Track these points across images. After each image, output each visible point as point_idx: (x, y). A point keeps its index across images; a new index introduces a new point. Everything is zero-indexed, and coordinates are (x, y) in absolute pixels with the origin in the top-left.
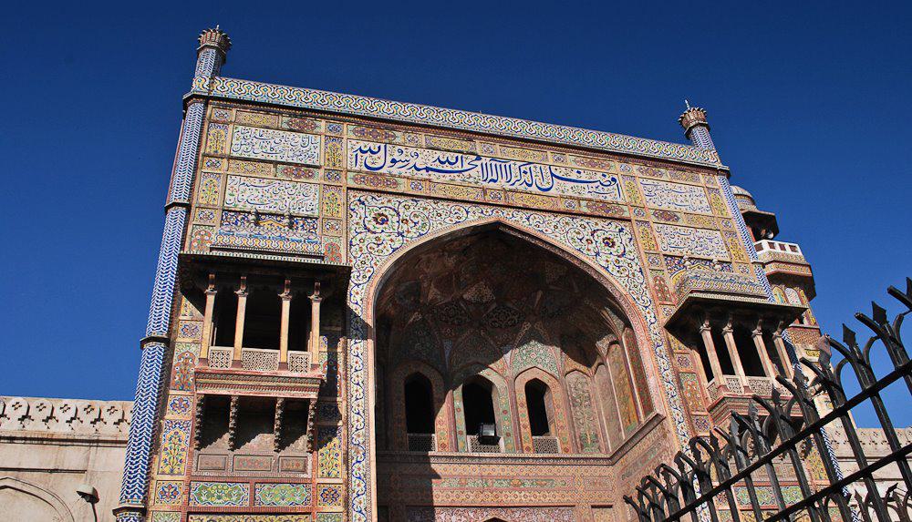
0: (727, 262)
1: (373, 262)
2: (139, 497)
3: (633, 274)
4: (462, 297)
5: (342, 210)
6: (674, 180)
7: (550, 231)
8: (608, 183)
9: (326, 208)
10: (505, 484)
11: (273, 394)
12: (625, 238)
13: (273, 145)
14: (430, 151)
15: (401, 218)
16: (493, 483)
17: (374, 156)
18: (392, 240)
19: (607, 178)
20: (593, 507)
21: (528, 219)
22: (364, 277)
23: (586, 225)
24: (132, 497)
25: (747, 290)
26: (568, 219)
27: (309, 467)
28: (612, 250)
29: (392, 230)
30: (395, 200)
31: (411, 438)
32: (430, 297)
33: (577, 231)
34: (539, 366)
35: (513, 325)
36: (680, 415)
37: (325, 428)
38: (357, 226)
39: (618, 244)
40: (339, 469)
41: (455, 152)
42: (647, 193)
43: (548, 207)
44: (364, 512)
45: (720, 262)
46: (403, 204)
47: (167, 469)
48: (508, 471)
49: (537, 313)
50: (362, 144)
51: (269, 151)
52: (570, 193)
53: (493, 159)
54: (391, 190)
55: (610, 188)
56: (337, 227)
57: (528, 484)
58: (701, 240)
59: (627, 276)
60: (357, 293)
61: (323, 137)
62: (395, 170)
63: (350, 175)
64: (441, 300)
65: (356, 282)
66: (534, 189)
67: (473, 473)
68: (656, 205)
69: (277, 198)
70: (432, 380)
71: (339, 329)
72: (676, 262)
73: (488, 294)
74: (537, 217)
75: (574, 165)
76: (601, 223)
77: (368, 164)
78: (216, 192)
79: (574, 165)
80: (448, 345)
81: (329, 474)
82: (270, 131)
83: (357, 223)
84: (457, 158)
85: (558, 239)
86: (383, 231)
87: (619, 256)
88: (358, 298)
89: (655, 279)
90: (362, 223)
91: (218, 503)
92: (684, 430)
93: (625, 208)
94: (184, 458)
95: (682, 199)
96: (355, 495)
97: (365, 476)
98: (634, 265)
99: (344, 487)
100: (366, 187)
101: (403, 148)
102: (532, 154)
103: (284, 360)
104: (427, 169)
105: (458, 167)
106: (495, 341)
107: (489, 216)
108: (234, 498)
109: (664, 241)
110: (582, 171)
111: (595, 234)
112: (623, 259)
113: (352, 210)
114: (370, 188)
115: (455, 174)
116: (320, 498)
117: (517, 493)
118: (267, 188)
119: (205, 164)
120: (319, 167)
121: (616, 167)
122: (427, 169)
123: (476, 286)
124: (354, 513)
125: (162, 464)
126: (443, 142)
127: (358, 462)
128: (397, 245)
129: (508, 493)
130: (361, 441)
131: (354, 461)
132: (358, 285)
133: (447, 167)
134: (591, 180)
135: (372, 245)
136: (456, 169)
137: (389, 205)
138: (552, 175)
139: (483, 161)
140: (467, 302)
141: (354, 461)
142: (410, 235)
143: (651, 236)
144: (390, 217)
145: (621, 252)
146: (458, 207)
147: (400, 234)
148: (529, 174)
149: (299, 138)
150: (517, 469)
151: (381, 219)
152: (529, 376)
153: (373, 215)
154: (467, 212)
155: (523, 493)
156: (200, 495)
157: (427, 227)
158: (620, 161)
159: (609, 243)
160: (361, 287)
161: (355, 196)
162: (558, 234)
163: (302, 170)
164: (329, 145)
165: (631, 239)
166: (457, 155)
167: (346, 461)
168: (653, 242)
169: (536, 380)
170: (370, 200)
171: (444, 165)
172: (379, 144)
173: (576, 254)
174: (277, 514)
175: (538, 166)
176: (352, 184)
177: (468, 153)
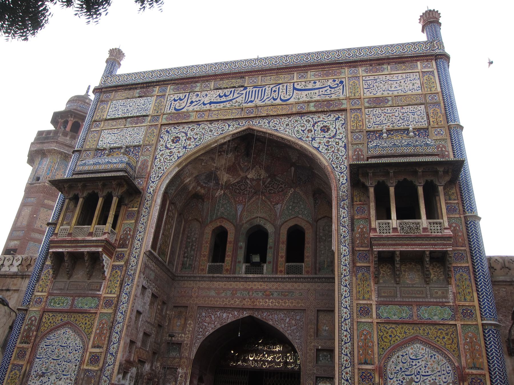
0: (423, 129)
1: (165, 167)
2: (26, 303)
3: (338, 150)
4: (246, 177)
5: (155, 139)
7: (282, 128)
8: (336, 85)
9: (147, 139)
10: (260, 294)
11: (82, 250)
12: (338, 124)
13: (129, 107)
14: (215, 91)
15: (188, 137)
16: (253, 293)
17: (181, 102)
18: (179, 152)
19: (336, 82)
20: (318, 311)
21: (269, 123)
23: (310, 119)
24: (24, 303)
25: (420, 150)
26: (298, 118)
27: (102, 288)
28: (326, 135)
29: (180, 146)
30: (187, 126)
31: (210, 266)
32: (225, 179)
33: (302, 125)
34: (300, 216)
35: (282, 191)
36: (347, 251)
37: (115, 266)
38: (161, 147)
40: (117, 289)
41: (230, 88)
42: (365, 87)
43: (284, 112)
44: (124, 313)
45: (418, 130)
46: (191, 128)
47: (40, 290)
48: (264, 286)
49: (294, 181)
50: (176, 96)
51: (126, 112)
52: (305, 99)
53: (255, 87)
54: (187, 121)
55: (338, 88)
56: (150, 149)
57: (275, 294)
58: (405, 114)
59: (333, 152)
60: (152, 187)
61: (155, 97)
62: (191, 108)
63: (165, 116)
64: (233, 180)
65: (153, 180)
66: (278, 101)
67: (242, 287)
68: (372, 94)
69: (124, 138)
70: (228, 230)
71: (136, 209)
72: (377, 136)
73: (263, 174)
74: (276, 120)
75: (313, 78)
76: (322, 116)
78: (95, 141)
79: (313, 78)
80: (240, 208)
81: (111, 291)
82: (129, 100)
83: (162, 145)
84: (231, 92)
85: (287, 133)
86: (175, 147)
87: (330, 138)
88: (152, 189)
89: (355, 150)
90: (165, 145)
91: (58, 307)
92: (347, 262)
93: (344, 102)
94: (48, 284)
95: (397, 85)
96: (122, 303)
97: (129, 293)
98: (340, 142)
99: (116, 299)
100: (171, 122)
101: (199, 93)
102: (283, 78)
103: (91, 231)
104: (210, 103)
106: (271, 202)
107: (243, 126)
108: (65, 305)
109: (372, 121)
110: (317, 81)
111: (316, 125)
112: (332, 140)
114: (173, 122)
115: (227, 103)
116: (104, 305)
117: (267, 300)
118: (119, 134)
119: (93, 127)
120: (147, 116)
121: (346, 72)
122: (210, 103)
123: (254, 169)
124: (119, 313)
125: (39, 287)
126: (225, 83)
127: (128, 285)
128: (181, 154)
129: (261, 300)
130: (132, 273)
131: (126, 285)
132: (153, 182)
133: (224, 99)
134: (324, 86)
135: (167, 156)
136: (228, 99)
137: (183, 130)
138: (294, 89)
139: (248, 90)
140: (252, 180)
141: (126, 285)
142: (190, 147)
143: (360, 119)
144: (181, 138)
145: (332, 135)
146: (224, 124)
147: (185, 147)
148: (277, 92)
149: (142, 100)
150: (270, 285)
151: (176, 140)
152: (291, 224)
153: (172, 138)
154: (229, 126)
155: (271, 300)
156: (50, 303)
157: (202, 140)
158: (350, 67)
159: (325, 129)
160: (154, 183)
161: (164, 129)
162: (288, 130)
163: (139, 118)
164: (158, 101)
166: (231, 89)
167: (121, 285)
168: (361, 124)
169: (296, 226)
170: (172, 129)
171: (222, 98)
172: (185, 94)
173: (297, 141)
174: (82, 313)
175: (285, 85)
176: (164, 122)
177: (239, 87)
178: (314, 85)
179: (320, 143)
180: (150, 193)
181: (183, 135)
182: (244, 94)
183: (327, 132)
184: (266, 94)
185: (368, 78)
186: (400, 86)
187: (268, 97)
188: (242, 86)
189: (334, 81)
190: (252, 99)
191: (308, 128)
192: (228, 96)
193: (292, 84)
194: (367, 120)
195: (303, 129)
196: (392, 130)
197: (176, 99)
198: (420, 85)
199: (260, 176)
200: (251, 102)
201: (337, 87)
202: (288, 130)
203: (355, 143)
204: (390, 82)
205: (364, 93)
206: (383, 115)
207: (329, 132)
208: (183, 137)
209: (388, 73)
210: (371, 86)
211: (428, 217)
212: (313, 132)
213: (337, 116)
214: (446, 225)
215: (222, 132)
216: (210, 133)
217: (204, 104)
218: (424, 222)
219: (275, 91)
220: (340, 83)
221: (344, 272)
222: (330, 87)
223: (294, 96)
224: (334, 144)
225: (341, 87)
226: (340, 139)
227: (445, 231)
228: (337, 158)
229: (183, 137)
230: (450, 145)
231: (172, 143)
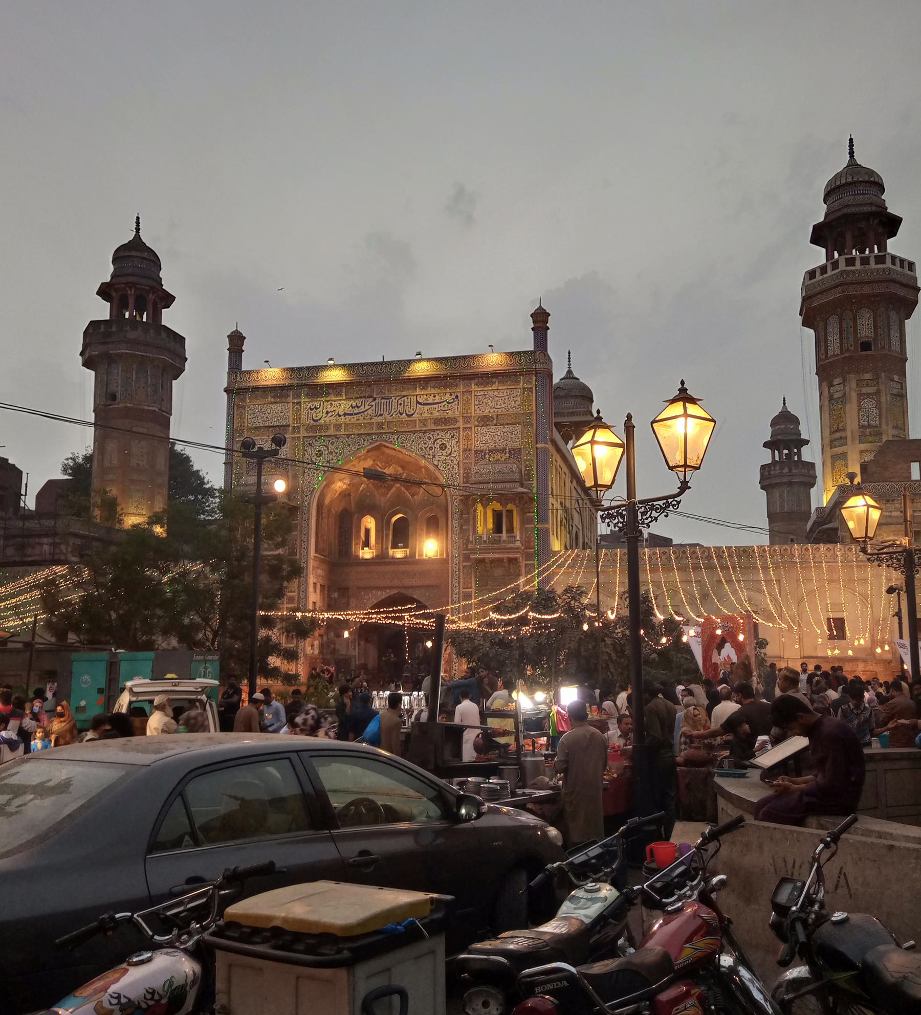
0: (517, 449)
3: (453, 468)
6: (500, 388)
7: (409, 445)
21: (397, 439)
22: (310, 491)
23: (431, 437)
39: (449, 447)
42: (476, 403)
52: (426, 415)
53: (383, 398)
58: (505, 434)
62: (327, 419)
68: (481, 412)
75: (433, 391)
76: (441, 433)
77: (314, 418)
85: (413, 450)
87: (447, 456)
88: (306, 503)
89: (465, 469)
95: (501, 402)
98: (455, 460)
104: (345, 414)
105: (362, 409)
109: (479, 439)
113: (306, 450)
115: (360, 415)
122: (345, 414)
136: (361, 411)
137: (324, 444)
138: (418, 402)
139: (377, 401)
145: (449, 452)
149: (278, 407)
154: (364, 440)
162: (413, 447)
165: (457, 442)
179: (439, 461)
181: (325, 448)
182: (374, 406)
183: (444, 450)
184: (393, 407)
185: (479, 394)
186: (504, 403)
188: (371, 397)
189: (451, 395)
190: (382, 412)
191: (430, 446)
192: (360, 407)
193: (415, 397)
194: (476, 439)
195: (426, 446)
196: (494, 450)
197: (312, 407)
198: (520, 403)
199: (397, 472)
200: (381, 415)
202: (413, 447)
203: (465, 461)
204: (497, 399)
205: (475, 410)
206: (488, 433)
207: (446, 450)
208: (325, 450)
209: (496, 388)
210: (481, 403)
211: (508, 532)
212: (433, 450)
213: (452, 435)
214: (518, 538)
217: (340, 416)
218: (504, 535)
219: (401, 404)
221: (455, 569)
222: (448, 402)
223: (417, 411)
224: (450, 462)
225: (456, 403)
226: (455, 457)
227: (517, 542)
228: (452, 476)
229: (325, 450)
230: (535, 465)
231: (315, 457)
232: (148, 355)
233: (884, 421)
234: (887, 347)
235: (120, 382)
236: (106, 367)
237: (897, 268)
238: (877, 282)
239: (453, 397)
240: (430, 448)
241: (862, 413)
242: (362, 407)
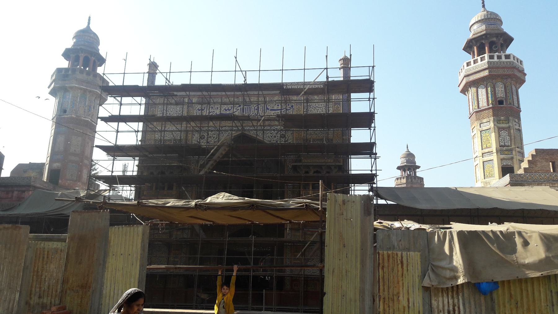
55: (290, 110)
83: (195, 140)
86: (203, 142)
139: (242, 107)
142: (211, 142)
178: (278, 107)
180: (192, 170)
184: (252, 111)
187: (253, 113)
191: (274, 135)
201: (289, 110)
204: (317, 108)
212: (276, 138)
215: (228, 134)
216: (222, 134)
219: (256, 109)
220: (291, 107)
225: (292, 110)
232: (88, 88)
233: (513, 142)
234: (512, 103)
235: (69, 102)
236: (63, 94)
237: (516, 61)
238: (507, 68)
239: (290, 106)
240: (274, 137)
241: (501, 138)
242: (232, 110)
